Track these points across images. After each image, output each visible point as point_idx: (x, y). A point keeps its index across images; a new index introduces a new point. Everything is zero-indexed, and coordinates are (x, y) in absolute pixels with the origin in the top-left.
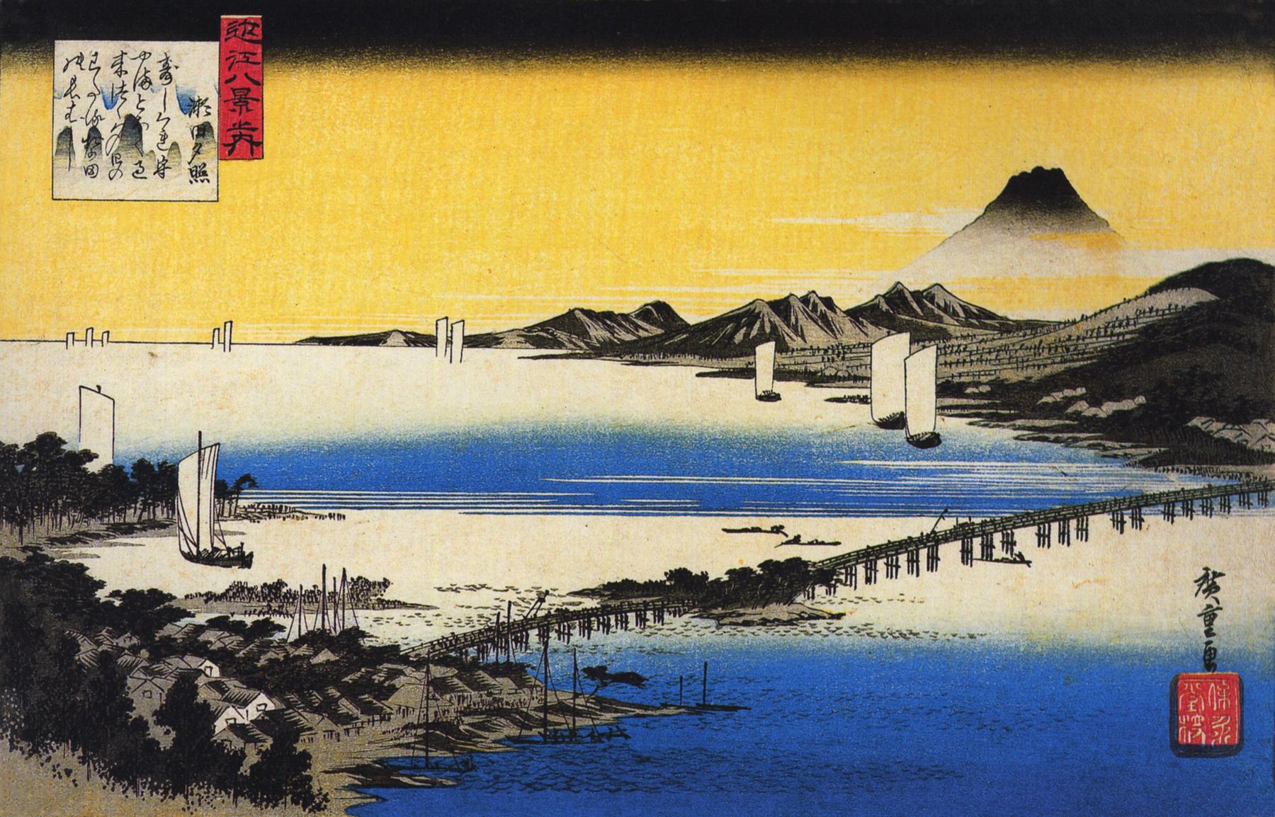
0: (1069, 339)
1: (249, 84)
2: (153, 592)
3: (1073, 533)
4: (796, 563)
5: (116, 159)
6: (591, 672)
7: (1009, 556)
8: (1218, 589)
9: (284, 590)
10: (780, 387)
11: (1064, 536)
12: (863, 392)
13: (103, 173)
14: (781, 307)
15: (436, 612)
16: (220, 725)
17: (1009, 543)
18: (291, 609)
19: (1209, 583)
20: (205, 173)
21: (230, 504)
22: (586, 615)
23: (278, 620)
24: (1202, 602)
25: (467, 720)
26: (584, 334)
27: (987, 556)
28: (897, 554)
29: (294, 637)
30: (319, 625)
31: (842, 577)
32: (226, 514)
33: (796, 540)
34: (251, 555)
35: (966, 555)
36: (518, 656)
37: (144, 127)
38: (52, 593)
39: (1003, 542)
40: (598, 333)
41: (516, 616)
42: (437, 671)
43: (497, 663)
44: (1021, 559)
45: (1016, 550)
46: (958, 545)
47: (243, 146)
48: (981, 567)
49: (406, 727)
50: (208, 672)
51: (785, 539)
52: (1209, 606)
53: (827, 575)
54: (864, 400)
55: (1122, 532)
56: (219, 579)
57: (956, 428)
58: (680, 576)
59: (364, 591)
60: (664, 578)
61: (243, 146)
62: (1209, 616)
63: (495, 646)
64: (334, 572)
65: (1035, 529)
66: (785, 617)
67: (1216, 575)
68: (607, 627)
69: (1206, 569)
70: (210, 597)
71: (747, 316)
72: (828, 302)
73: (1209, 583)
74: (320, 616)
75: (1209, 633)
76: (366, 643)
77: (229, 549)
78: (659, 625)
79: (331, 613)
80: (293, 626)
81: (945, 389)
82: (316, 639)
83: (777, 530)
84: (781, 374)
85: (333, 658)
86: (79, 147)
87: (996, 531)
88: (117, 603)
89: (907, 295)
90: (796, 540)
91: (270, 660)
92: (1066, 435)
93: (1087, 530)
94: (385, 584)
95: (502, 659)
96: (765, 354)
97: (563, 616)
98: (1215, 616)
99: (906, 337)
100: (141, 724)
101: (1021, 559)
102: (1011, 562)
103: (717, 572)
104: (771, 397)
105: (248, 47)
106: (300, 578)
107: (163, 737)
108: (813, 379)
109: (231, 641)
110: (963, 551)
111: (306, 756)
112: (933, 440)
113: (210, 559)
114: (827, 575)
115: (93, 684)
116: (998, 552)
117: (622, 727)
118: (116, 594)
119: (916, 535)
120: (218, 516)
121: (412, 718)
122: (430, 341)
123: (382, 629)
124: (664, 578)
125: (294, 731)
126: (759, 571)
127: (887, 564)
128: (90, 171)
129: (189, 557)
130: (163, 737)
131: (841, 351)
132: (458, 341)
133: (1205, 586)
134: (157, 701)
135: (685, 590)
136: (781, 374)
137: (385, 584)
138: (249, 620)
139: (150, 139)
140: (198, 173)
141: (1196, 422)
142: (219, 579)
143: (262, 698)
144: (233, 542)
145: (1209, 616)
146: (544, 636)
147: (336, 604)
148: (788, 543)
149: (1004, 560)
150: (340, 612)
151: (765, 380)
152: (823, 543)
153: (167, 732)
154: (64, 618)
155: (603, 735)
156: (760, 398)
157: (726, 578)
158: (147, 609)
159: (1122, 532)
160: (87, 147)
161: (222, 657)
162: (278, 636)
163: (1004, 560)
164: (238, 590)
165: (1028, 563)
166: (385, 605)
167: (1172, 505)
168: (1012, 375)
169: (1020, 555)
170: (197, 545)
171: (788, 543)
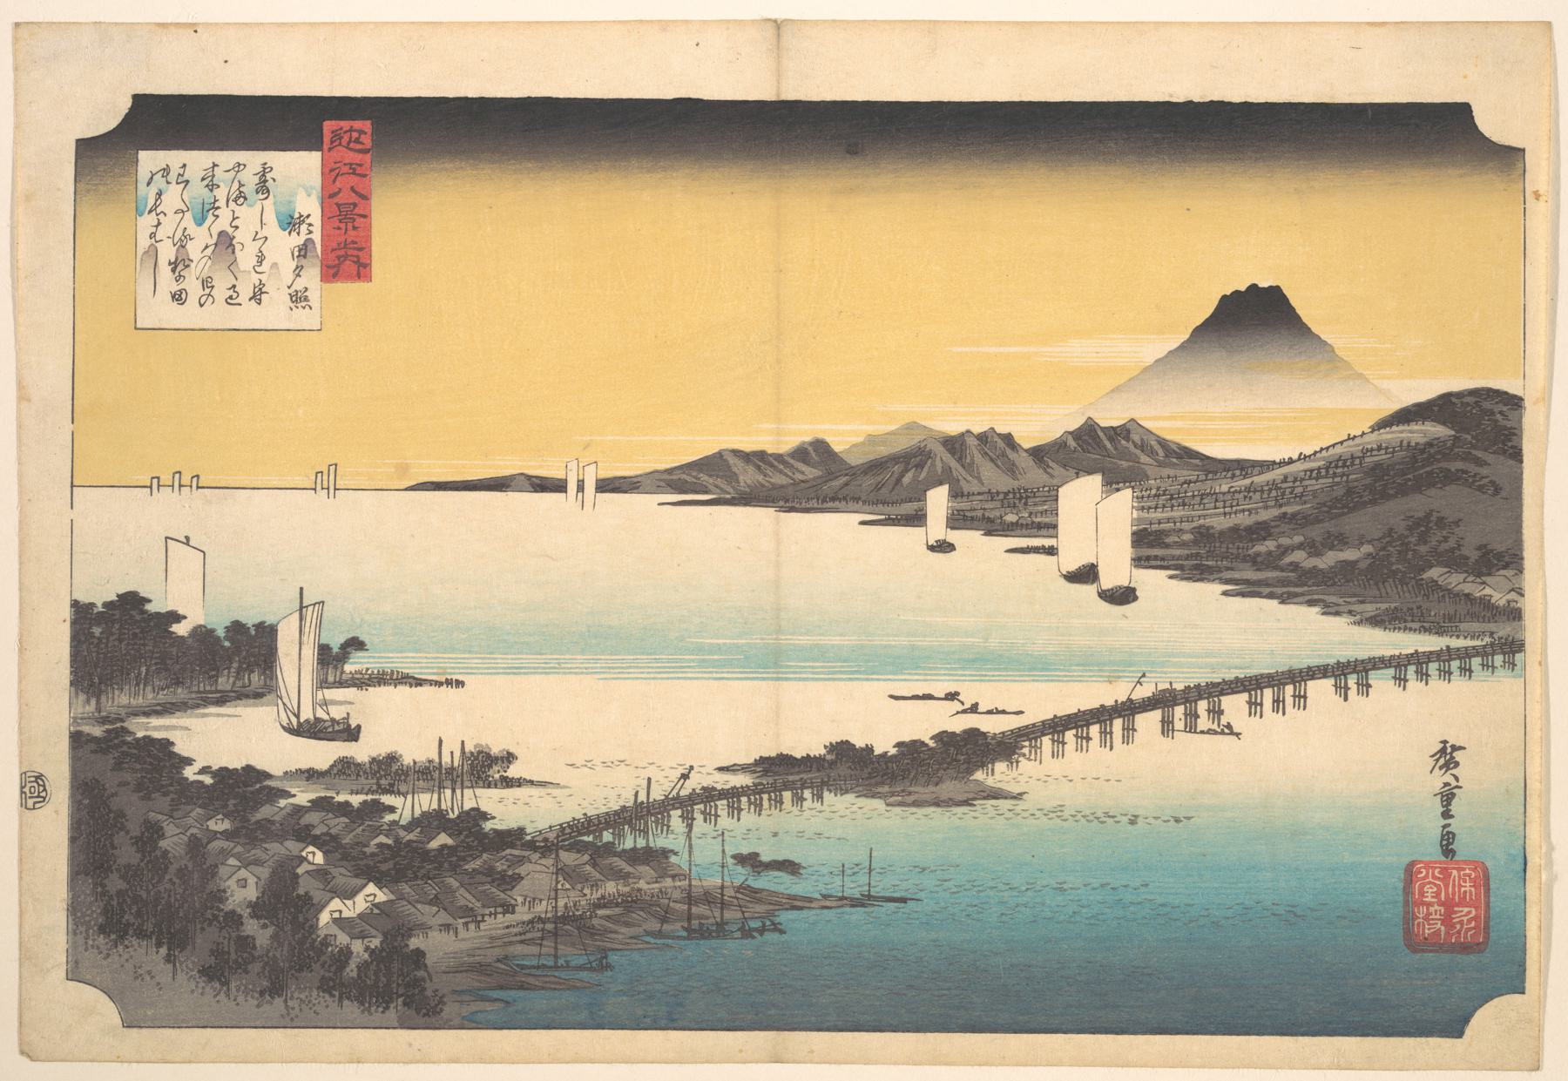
0: (1285, 480)
1: (354, 198)
2: (249, 769)
3: (1289, 700)
4: (973, 734)
5: (207, 283)
6: (741, 859)
7: (1215, 727)
8: (1457, 764)
9: (395, 767)
10: (954, 536)
11: (1278, 703)
12: (1047, 542)
13: (193, 300)
14: (954, 444)
15: (567, 792)
16: (324, 918)
17: (1216, 712)
18: (403, 788)
19: (1447, 756)
20: (306, 299)
21: (336, 668)
22: (732, 794)
23: (387, 799)
24: (1438, 780)
25: (600, 912)
26: (732, 477)
27: (1191, 728)
28: (1088, 725)
29: (406, 818)
30: (435, 806)
31: (1026, 751)
32: (331, 679)
33: (974, 709)
34: (359, 727)
35: (1167, 726)
36: (660, 842)
37: (238, 247)
38: (135, 771)
39: (1209, 711)
40: (748, 477)
41: (657, 794)
42: (567, 858)
43: (634, 849)
44: (1229, 730)
45: (1224, 721)
46: (1156, 715)
47: (349, 266)
48: (1182, 737)
49: (531, 922)
50: (310, 857)
51: (960, 708)
52: (1446, 784)
53: (1007, 747)
54: (1051, 551)
55: (1346, 699)
56: (322, 754)
57: (1153, 583)
58: (842, 750)
59: (484, 767)
60: (823, 752)
61: (349, 266)
62: (1447, 796)
63: (633, 829)
64: (452, 748)
65: (1245, 696)
66: (965, 797)
67: (1455, 748)
68: (759, 807)
69: (1445, 742)
70: (311, 775)
71: (915, 458)
72: (1008, 439)
73: (1447, 756)
74: (436, 796)
75: (1446, 814)
76: (488, 826)
77: (333, 720)
78: (817, 805)
79: (448, 792)
80: (406, 807)
81: (1141, 538)
82: (434, 821)
83: (952, 696)
84: (958, 520)
85: (450, 841)
86: (165, 271)
87: (1201, 698)
88: (207, 780)
89: (1101, 434)
90: (974, 709)
91: (381, 845)
92: (1279, 590)
93: (1305, 697)
94: (509, 758)
95: (641, 843)
96: (938, 501)
97: (709, 795)
98: (1454, 795)
99: (1096, 480)
100: (234, 919)
101: (1229, 730)
102: (1216, 733)
103: (884, 745)
104: (943, 547)
105: (358, 158)
106: (414, 752)
107: (258, 932)
108: (993, 528)
109: (338, 824)
110: (1163, 721)
111: (419, 954)
112: (1123, 596)
113: (313, 730)
114: (1007, 747)
115: (181, 872)
116: (1204, 722)
117: (777, 920)
118: (204, 770)
119: (1109, 702)
120: (323, 684)
121: (540, 908)
122: (559, 486)
123: (503, 809)
124: (823, 752)
125: (408, 931)
126: (932, 744)
127: (1076, 736)
128: (178, 297)
129: (290, 730)
130: (258, 932)
131: (1021, 497)
132: (590, 486)
133: (1442, 761)
134: (251, 893)
135: (848, 767)
136: (958, 520)
137: (509, 758)
138: (356, 800)
139: (246, 258)
140: (298, 298)
141: (1434, 573)
142: (322, 754)
143: (371, 888)
144: (337, 713)
145: (1447, 796)
146: (689, 820)
147: (454, 782)
148: (964, 712)
149: (1209, 732)
150: (458, 792)
151: (936, 525)
152: (1004, 712)
153: (264, 926)
154: (147, 798)
155: (756, 930)
156: (932, 548)
157: (893, 751)
158: (242, 788)
159: (1346, 699)
160: (173, 271)
161: (327, 843)
162: (389, 818)
163: (1209, 732)
164: (345, 767)
165: (1238, 735)
166: (508, 783)
167: (1399, 666)
168: (1220, 523)
169: (1229, 726)
170: (297, 716)
171: (964, 712)
